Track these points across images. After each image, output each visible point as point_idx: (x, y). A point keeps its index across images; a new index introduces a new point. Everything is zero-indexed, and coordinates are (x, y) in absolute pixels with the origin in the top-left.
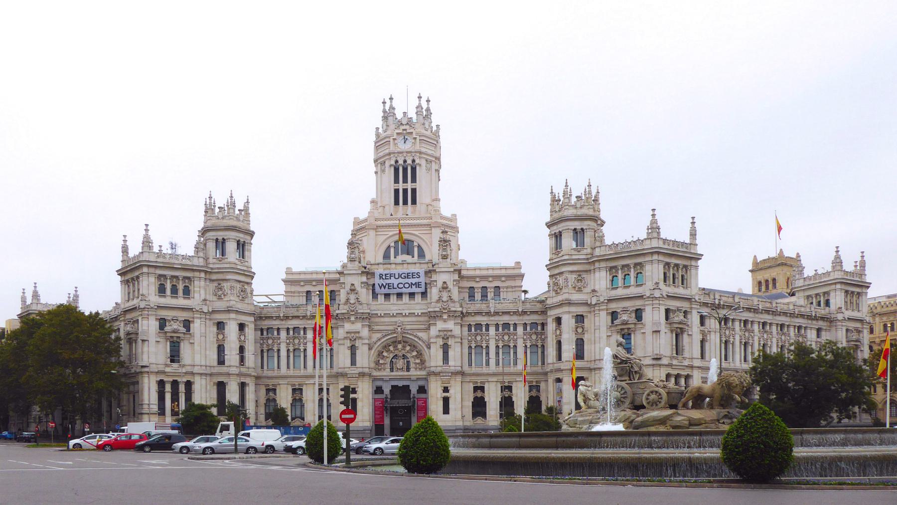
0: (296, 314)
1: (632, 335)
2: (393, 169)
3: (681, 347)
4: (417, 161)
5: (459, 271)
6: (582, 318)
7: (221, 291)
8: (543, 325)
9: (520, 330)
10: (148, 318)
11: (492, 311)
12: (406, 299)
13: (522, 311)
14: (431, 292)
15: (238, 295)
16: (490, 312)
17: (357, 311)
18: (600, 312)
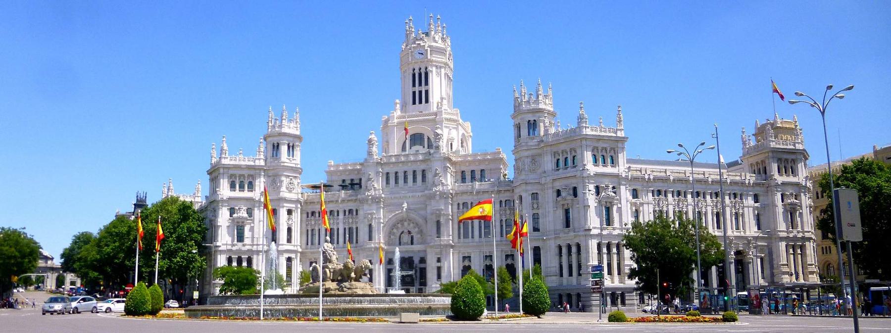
0: (331, 199)
1: (570, 209)
4: (430, 68)
13: (498, 191)
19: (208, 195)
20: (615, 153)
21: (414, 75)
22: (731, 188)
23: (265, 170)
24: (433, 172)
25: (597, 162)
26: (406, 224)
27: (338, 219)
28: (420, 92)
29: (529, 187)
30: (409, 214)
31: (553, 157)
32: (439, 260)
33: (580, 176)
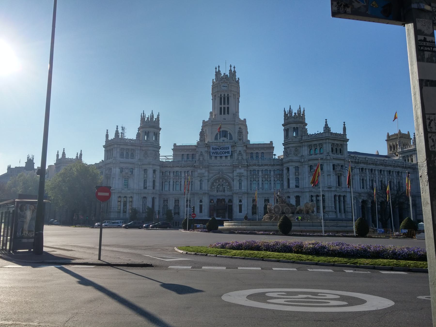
0: (177, 165)
2: (219, 98)
3: (341, 182)
5: (246, 146)
6: (298, 168)
7: (147, 155)
8: (283, 170)
9: (272, 173)
10: (116, 168)
11: (260, 164)
12: (224, 158)
14: (234, 155)
15: (154, 157)
16: (259, 165)
17: (203, 164)
18: (305, 166)
19: (103, 160)
20: (342, 147)
21: (221, 99)
22: (397, 169)
23: (140, 146)
24: (237, 152)
25: (334, 152)
26: (221, 180)
27: (181, 176)
28: (224, 108)
29: (294, 164)
30: (223, 175)
31: (308, 148)
32: (240, 201)
33: (325, 159)
